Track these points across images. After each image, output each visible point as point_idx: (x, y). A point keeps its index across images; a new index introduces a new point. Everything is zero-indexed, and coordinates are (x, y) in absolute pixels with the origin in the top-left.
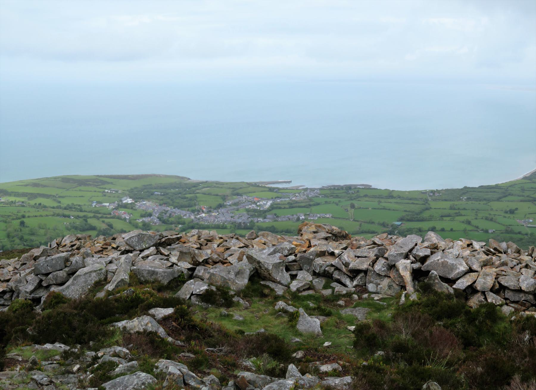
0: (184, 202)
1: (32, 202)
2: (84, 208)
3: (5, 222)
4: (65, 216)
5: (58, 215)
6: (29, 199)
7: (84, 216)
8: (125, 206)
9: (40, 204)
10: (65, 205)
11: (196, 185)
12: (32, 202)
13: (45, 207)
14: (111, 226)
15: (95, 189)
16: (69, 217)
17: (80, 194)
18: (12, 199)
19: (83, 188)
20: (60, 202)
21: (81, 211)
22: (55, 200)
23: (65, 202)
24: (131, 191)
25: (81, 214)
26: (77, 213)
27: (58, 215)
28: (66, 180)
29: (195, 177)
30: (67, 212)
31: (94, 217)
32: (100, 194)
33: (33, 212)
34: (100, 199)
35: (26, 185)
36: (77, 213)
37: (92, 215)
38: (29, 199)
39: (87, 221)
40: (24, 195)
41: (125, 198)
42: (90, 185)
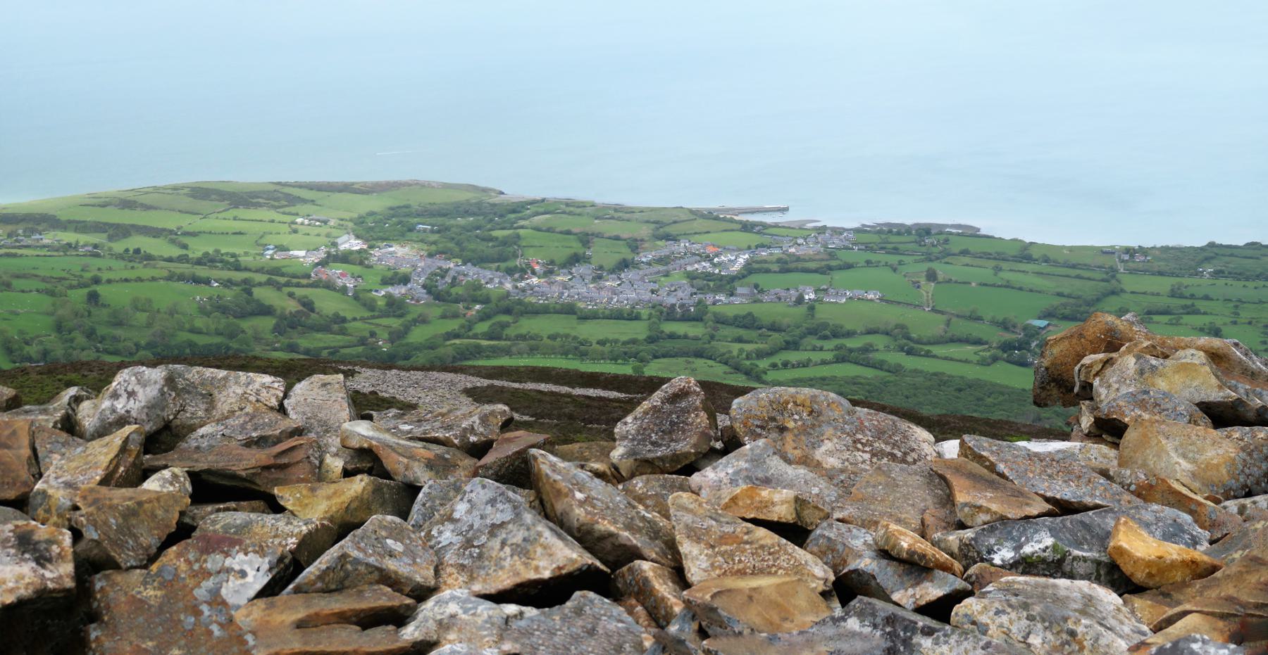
0: (487, 248)
1: (119, 247)
3: (51, 293)
4: (197, 280)
5: (181, 278)
6: (111, 238)
7: (245, 281)
8: (345, 258)
9: (137, 251)
10: (199, 254)
11: (518, 208)
12: (119, 247)
13: (149, 257)
14: (308, 305)
15: (272, 214)
16: (207, 282)
17: (238, 226)
18: (68, 237)
20: (185, 247)
21: (238, 268)
22: (173, 242)
23: (198, 248)
24: (360, 221)
25: (238, 276)
26: (226, 274)
27: (181, 278)
28: (201, 193)
29: (517, 188)
30: (202, 272)
31: (269, 283)
32: (285, 228)
33: (120, 270)
34: (285, 239)
35: (104, 206)
36: (226, 274)
37: (262, 278)
38: (111, 238)
39: (250, 293)
40: (98, 227)
41: (345, 237)
42: (258, 205)
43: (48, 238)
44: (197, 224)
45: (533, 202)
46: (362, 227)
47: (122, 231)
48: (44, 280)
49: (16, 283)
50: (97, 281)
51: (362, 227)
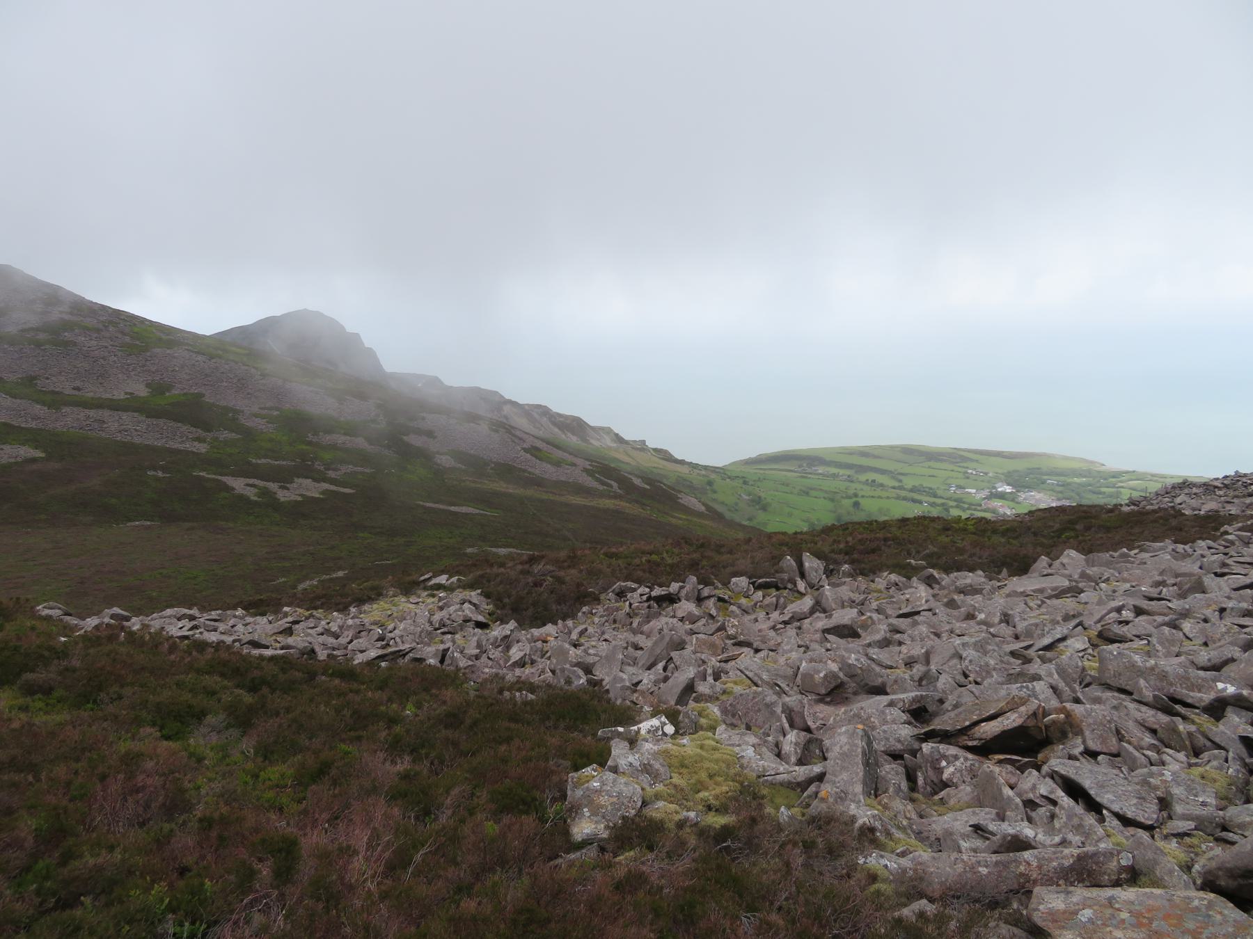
1: (863, 478)
2: (940, 493)
3: (832, 500)
4: (914, 501)
5: (905, 499)
7: (943, 504)
8: (1002, 496)
9: (874, 481)
10: (909, 486)
12: (863, 478)
13: (882, 485)
15: (951, 467)
16: (920, 502)
18: (834, 470)
19: (932, 464)
20: (900, 481)
21: (935, 496)
22: (893, 478)
23: (909, 482)
25: (939, 501)
26: (932, 500)
27: (905, 499)
28: (908, 451)
30: (916, 496)
31: (957, 507)
32: (960, 475)
33: (867, 491)
34: (962, 482)
35: (851, 454)
36: (932, 500)
37: (954, 504)
39: (947, 510)
42: (941, 461)
43: (821, 470)
44: (907, 469)
45: (1127, 472)
46: (1009, 478)
47: (862, 469)
48: (826, 492)
49: (813, 493)
50: (856, 495)
51: (1009, 478)
